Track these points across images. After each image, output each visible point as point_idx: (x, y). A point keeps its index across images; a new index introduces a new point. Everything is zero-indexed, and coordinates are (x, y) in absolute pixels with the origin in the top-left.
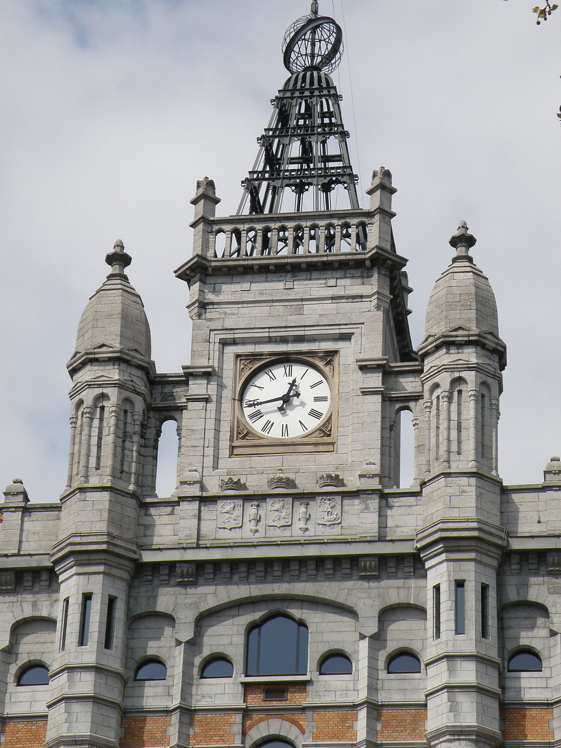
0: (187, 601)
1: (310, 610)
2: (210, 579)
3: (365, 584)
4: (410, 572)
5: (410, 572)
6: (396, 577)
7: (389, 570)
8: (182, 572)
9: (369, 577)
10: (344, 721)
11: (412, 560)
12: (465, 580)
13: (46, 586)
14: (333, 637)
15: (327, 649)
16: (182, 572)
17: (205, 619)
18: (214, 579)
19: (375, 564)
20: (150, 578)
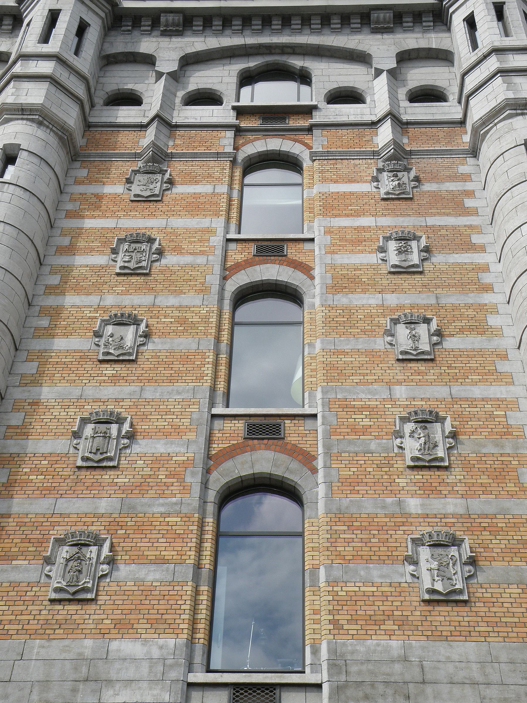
0: (170, 46)
1: (313, 61)
2: (199, 31)
3: (379, 36)
4: (430, 26)
5: (430, 26)
6: (412, 31)
7: (405, 25)
8: (167, 21)
9: (383, 31)
10: (361, 137)
11: (431, 15)
12: (504, 3)
13: (8, 30)
14: (342, 78)
15: (335, 86)
16: (167, 21)
17: (190, 61)
18: (203, 30)
19: (390, 15)
20: (130, 28)
